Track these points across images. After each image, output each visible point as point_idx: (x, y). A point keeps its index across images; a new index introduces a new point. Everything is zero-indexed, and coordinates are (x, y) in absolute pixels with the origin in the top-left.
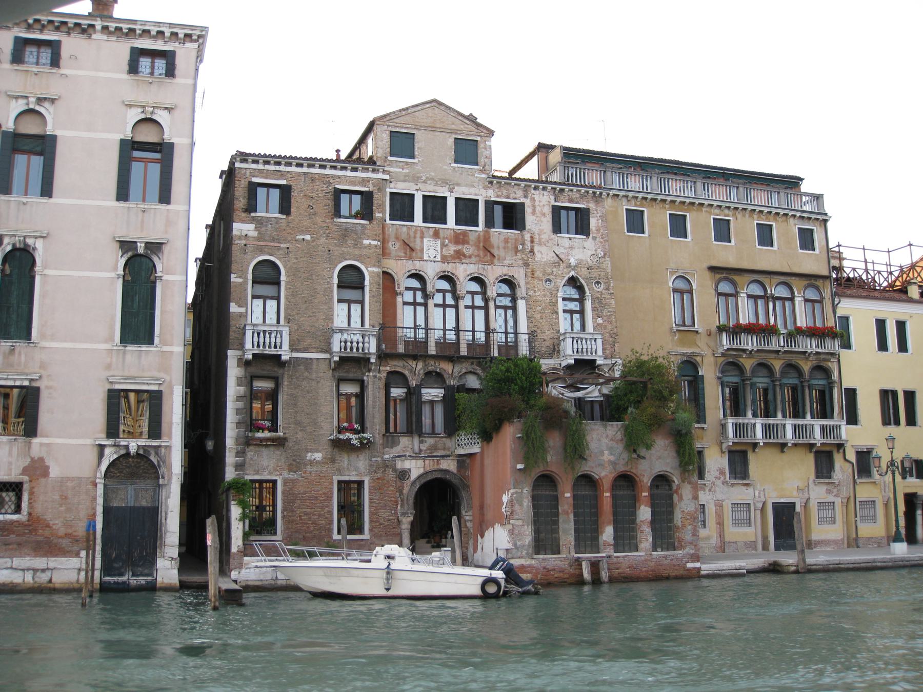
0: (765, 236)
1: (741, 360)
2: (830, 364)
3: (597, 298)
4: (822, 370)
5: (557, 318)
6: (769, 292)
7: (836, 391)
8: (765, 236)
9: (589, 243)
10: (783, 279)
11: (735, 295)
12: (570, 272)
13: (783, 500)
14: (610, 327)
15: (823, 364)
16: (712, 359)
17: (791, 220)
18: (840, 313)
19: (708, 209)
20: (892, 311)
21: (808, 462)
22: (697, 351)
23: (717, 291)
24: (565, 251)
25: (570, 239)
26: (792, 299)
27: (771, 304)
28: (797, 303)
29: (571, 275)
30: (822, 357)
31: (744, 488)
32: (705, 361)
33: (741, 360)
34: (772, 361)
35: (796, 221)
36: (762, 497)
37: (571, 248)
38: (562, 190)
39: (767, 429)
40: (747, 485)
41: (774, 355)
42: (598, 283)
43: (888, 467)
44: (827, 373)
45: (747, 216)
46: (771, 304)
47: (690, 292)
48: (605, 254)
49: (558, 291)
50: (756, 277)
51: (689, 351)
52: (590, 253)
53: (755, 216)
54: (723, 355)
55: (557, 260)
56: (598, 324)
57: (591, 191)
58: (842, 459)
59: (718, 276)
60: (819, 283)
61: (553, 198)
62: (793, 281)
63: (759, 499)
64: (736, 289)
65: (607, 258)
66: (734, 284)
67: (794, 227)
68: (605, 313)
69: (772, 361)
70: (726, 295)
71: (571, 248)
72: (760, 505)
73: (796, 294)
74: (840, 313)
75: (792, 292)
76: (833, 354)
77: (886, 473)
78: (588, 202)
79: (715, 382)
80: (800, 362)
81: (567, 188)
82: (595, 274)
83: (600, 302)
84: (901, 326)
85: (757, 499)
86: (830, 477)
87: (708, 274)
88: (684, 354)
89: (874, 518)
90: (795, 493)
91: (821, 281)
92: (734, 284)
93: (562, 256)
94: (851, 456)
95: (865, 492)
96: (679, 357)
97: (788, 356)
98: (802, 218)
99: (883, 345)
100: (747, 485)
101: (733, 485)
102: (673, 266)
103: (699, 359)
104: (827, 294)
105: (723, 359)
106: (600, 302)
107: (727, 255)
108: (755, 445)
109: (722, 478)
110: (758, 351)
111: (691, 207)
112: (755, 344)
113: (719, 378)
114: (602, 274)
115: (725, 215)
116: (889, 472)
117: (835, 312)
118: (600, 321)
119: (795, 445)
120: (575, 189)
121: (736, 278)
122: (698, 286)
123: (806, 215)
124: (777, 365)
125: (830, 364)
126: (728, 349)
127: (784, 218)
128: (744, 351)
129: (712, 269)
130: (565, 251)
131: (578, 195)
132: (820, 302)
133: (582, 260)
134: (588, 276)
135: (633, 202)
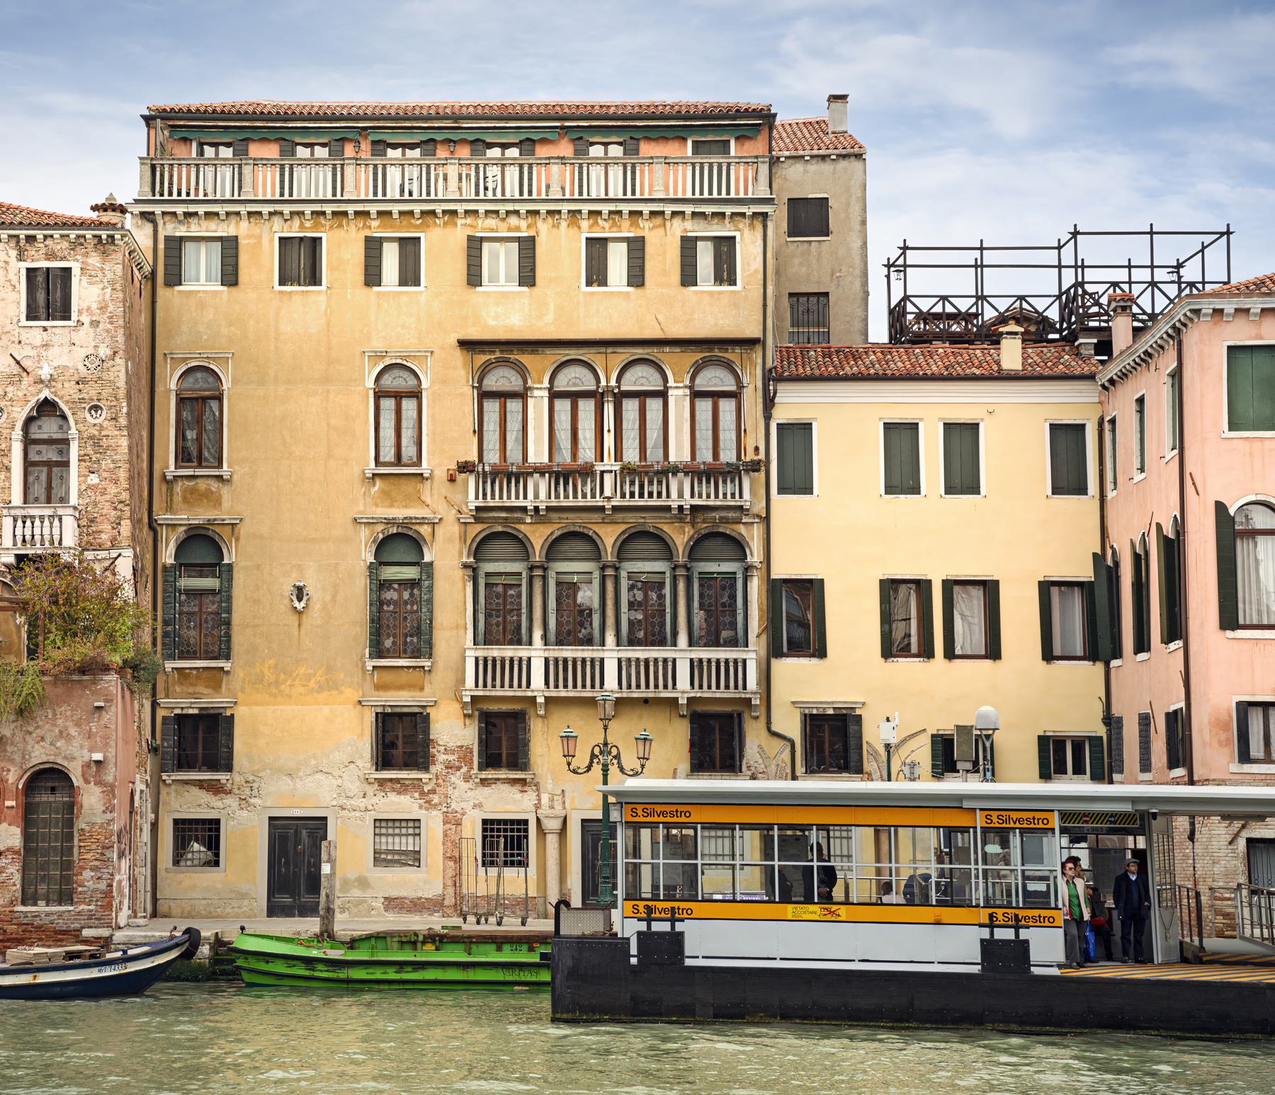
1: (522, 527)
2: (742, 529)
3: (92, 437)
5: (8, 478)
6: (603, 383)
7: (755, 586)
9: (85, 336)
10: (639, 352)
11: (522, 396)
12: (40, 391)
14: (112, 490)
16: (456, 529)
18: (782, 414)
19: (469, 221)
20: (931, 407)
23: (479, 388)
24: (33, 353)
25: (45, 329)
26: (663, 394)
27: (609, 409)
28: (671, 401)
29: (42, 396)
30: (717, 515)
32: (440, 531)
33: (522, 527)
36: (558, 806)
37: (46, 346)
38: (31, 239)
40: (523, 782)
41: (596, 517)
42: (96, 408)
43: (593, 756)
44: (738, 547)
45: (564, 224)
46: (609, 409)
47: (416, 395)
48: (115, 353)
49: (13, 428)
50: (573, 353)
51: (399, 513)
52: (83, 353)
53: (585, 224)
54: (478, 520)
55: (16, 370)
56: (89, 487)
57: (89, 234)
58: (764, 733)
59: (481, 359)
60: (732, 355)
61: (13, 253)
62: (667, 357)
63: (550, 812)
64: (525, 381)
65: (117, 359)
66: (523, 372)
68: (106, 464)
70: (503, 396)
71: (46, 346)
72: (552, 825)
73: (671, 383)
74: (782, 414)
75: (665, 380)
77: (589, 768)
78: (87, 255)
79: (459, 574)
80: (666, 528)
81: (39, 234)
82: (91, 392)
83: (97, 445)
84: (962, 438)
87: (458, 356)
88: (389, 522)
91: (738, 350)
92: (523, 372)
93: (25, 363)
94: (790, 724)
97: (633, 518)
99: (902, 479)
100: (523, 782)
101: (484, 782)
102: (378, 345)
103: (425, 530)
104: (753, 381)
105: (479, 527)
106: (97, 445)
107: (505, 310)
109: (464, 769)
110: (548, 509)
111: (430, 220)
112: (543, 495)
113: (465, 566)
114: (104, 395)
115: (510, 230)
116: (597, 768)
117: (768, 418)
118: (93, 479)
120: (56, 234)
121: (526, 359)
122: (433, 382)
123: (709, 209)
125: (742, 529)
126: (478, 509)
127: (658, 220)
128: (524, 509)
129: (467, 345)
130: (33, 353)
131: (65, 245)
132: (735, 395)
133: (66, 367)
134: (77, 396)
135: (296, 222)
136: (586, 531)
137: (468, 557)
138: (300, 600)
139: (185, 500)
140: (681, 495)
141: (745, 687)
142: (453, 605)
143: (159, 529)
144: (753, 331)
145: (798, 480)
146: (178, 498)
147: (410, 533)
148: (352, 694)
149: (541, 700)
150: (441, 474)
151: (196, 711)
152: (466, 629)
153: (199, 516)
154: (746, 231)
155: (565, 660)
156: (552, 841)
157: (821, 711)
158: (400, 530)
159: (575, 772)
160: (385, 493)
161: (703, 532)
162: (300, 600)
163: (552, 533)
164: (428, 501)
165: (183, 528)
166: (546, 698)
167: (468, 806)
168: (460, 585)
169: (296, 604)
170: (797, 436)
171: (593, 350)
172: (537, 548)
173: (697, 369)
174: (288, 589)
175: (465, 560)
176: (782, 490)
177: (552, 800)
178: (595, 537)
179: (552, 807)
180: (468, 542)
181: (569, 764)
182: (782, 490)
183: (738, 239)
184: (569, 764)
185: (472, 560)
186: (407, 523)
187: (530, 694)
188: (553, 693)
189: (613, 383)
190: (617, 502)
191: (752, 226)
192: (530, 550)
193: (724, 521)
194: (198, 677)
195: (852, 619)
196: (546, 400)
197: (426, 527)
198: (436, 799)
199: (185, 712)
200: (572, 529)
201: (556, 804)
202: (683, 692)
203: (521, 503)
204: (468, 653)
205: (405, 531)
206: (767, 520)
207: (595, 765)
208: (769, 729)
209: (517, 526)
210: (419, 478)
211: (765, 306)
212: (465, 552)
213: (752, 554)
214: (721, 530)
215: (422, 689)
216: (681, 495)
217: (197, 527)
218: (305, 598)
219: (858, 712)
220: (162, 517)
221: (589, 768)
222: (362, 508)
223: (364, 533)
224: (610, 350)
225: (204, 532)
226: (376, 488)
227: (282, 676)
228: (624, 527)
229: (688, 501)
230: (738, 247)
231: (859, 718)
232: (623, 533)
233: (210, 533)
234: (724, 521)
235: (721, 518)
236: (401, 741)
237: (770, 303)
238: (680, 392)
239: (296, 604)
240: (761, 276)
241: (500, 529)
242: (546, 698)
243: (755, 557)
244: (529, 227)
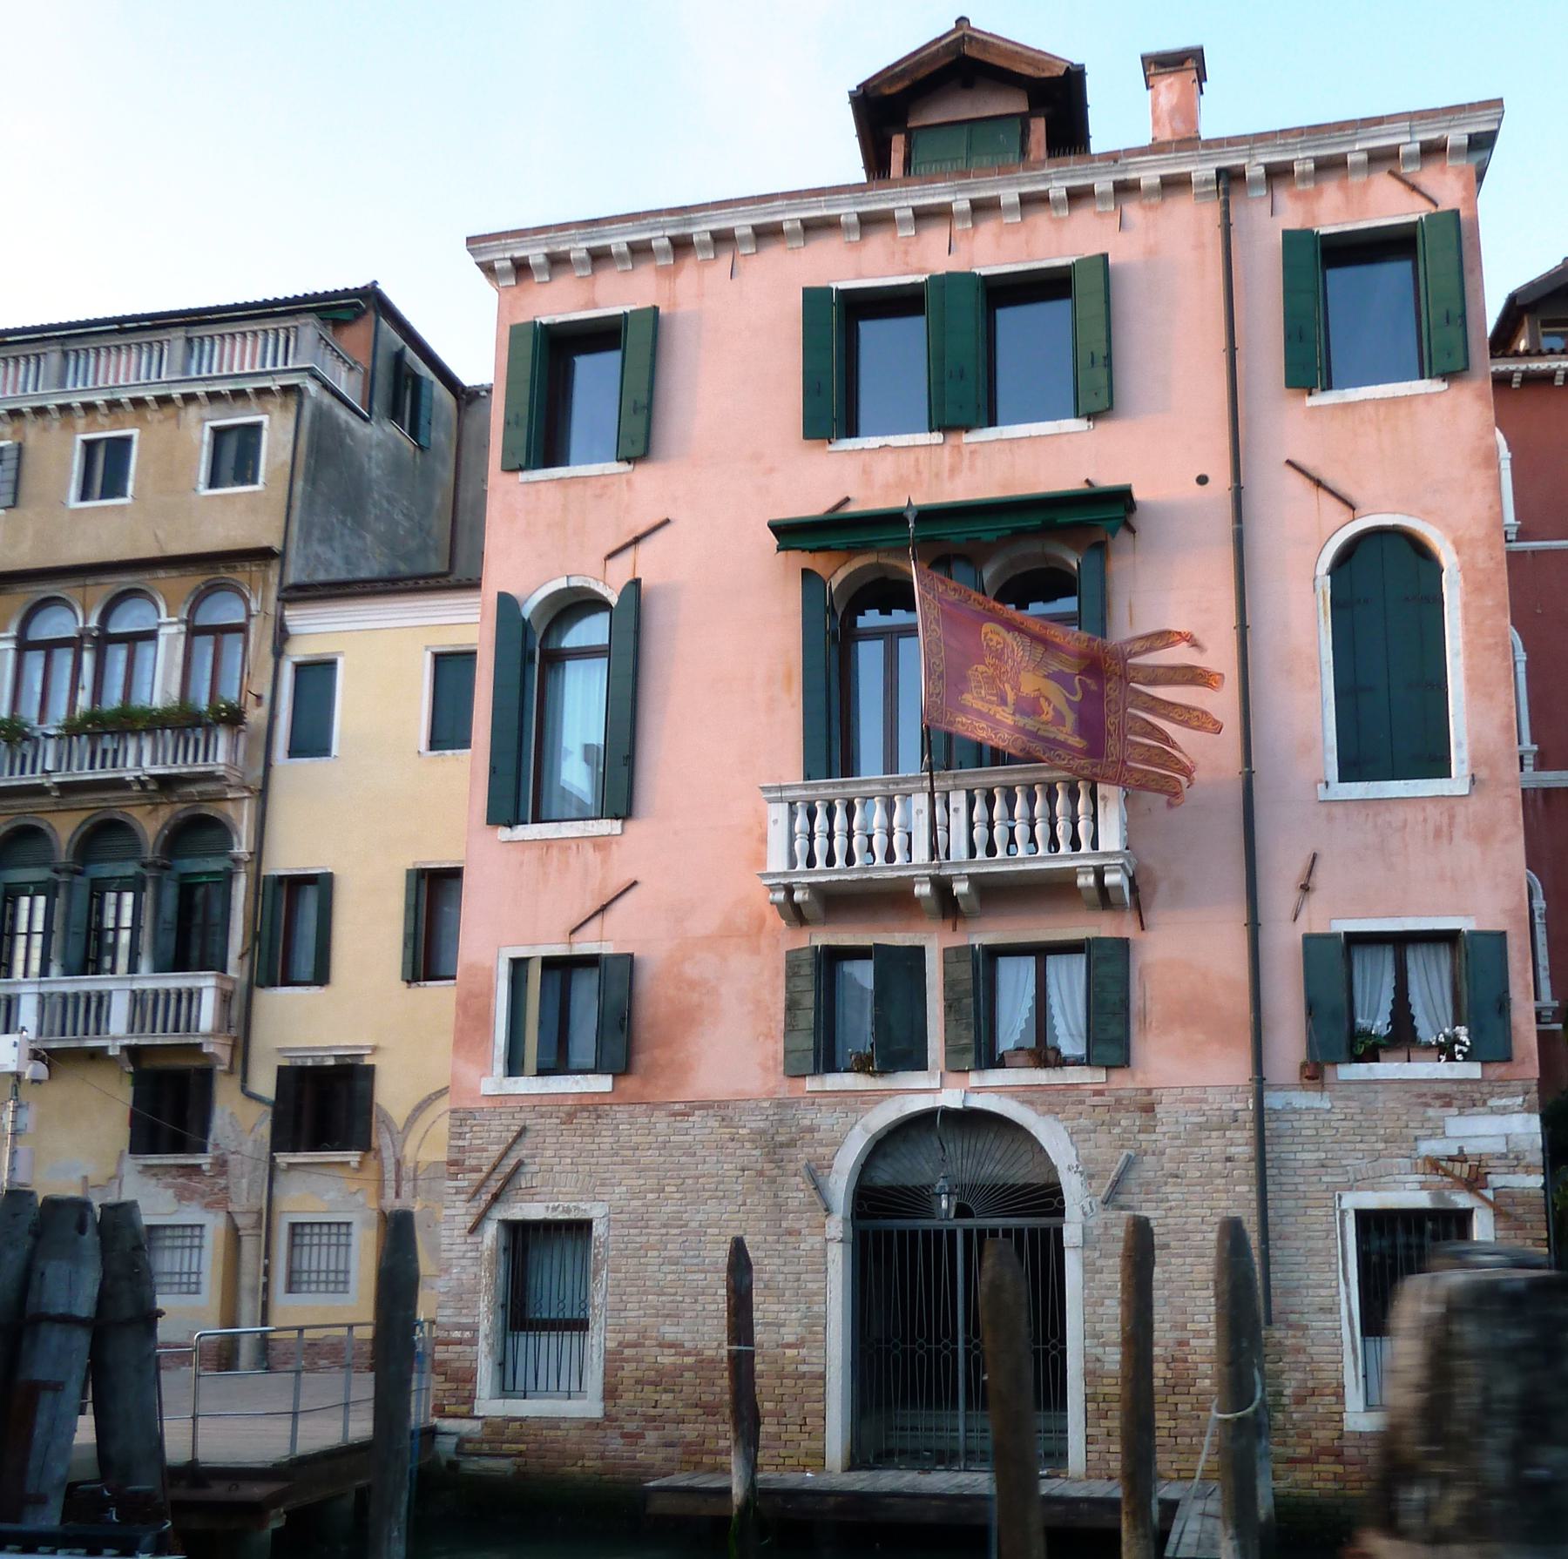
0: (106, 469)
2: (229, 808)
4: (199, 830)
7: (240, 888)
8: (106, 469)
15: (209, 810)
17: (193, 412)
18: (299, 651)
21: (108, 1108)
27: (88, 659)
30: (193, 789)
34: (49, 818)
35: (207, 411)
46: (88, 659)
53: (81, 423)
58: (239, 1096)
67: (199, 428)
74: (299, 651)
89: (338, 1281)
95: (322, 1190)
98: (213, 397)
117: (278, 653)
123: (224, 387)
127: (169, 410)
140: (139, 763)
144: (272, 540)
145: (312, 738)
154: (277, 413)
157: (318, 1062)
170: (316, 678)
171: (72, 583)
173: (200, 598)
183: (266, 425)
189: (93, 623)
191: (284, 406)
195: (369, 929)
196: (11, 656)
202: (114, 1038)
208: (243, 1089)
211: (289, 507)
213: (240, 843)
214: (204, 811)
216: (139, 763)
219: (367, 1061)
224: (90, 581)
228: (84, 815)
230: (265, 435)
231: (370, 1071)
232: (83, 823)
235: (201, 793)
237: (297, 503)
238: (173, 630)
240: (288, 470)
243: (242, 846)
244: (15, 432)
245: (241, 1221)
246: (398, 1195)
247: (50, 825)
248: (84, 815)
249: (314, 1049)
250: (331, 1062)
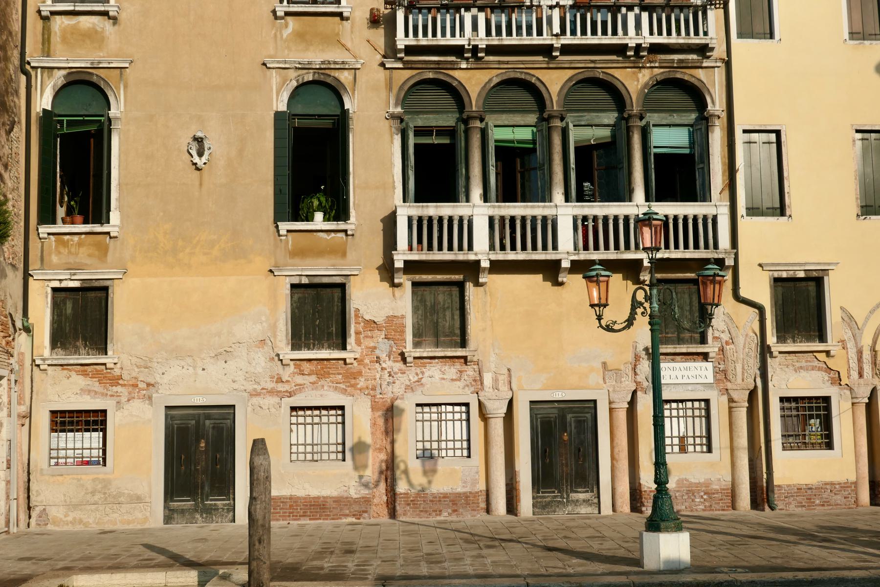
1: (456, 74)
2: (701, 74)
13: (559, 396)
22: (335, 55)
31: (451, 370)
33: (456, 74)
34: (538, 74)
39: (505, 231)
44: (696, 96)
51: (316, 56)
69: (538, 74)
76: (703, 50)
77: (630, 322)
80: (617, 73)
85: (487, 394)
86: (703, 340)
88: (305, 67)
90: (596, 378)
96: (292, 74)
103: (345, 77)
105: (408, 73)
108: (472, 269)
113: (393, 117)
119: (578, 267)
124: (554, 81)
125: (701, 74)
128: (458, 51)
136: (528, 78)
137: (396, 105)
138: (200, 154)
139: (64, 39)
141: (716, 246)
142: (377, 163)
143: (33, 73)
146: (56, 39)
147: (329, 80)
148: (262, 263)
149: (485, 264)
150: (361, 16)
151: (76, 284)
152: (394, 188)
153: (81, 60)
155: (513, 219)
156: (497, 428)
158: (317, 77)
159: (609, 329)
160: (300, 36)
161: (659, 78)
162: (200, 154)
163: (490, 80)
164: (349, 45)
165: (64, 72)
166: (491, 262)
167: (398, 389)
168: (387, 137)
169: (196, 159)
172: (474, 96)
174: (185, 139)
175: (391, 110)
176: (740, 35)
177: (496, 380)
178: (538, 84)
179: (496, 388)
180: (395, 90)
181: (599, 318)
182: (740, 35)
184: (599, 318)
185: (399, 110)
186: (325, 68)
187: (472, 257)
188: (500, 256)
190: (568, 40)
192: (466, 99)
193: (683, 65)
194: (80, 244)
197: (346, 73)
198: (362, 383)
199: (65, 284)
200: (512, 75)
201: (501, 383)
203: (457, 41)
204: (399, 212)
205: (322, 78)
206: (728, 64)
207: (639, 317)
208: (737, 297)
209: (451, 72)
210: (338, 19)
212: (392, 101)
214: (678, 76)
215: (344, 255)
217: (80, 71)
218: (206, 153)
220: (34, 58)
221: (630, 322)
222: (272, 52)
223: (274, 78)
225: (87, 78)
226: (290, 29)
227: (180, 243)
228: (571, 73)
229: (647, 39)
232: (570, 79)
233: (94, 79)
234: (683, 65)
236: (320, 314)
239: (196, 159)
241: (431, 75)
242: (491, 262)
243: (716, 105)
245: (735, 395)
246: (861, 375)
247: (538, 79)
248: (571, 73)
249: (805, 264)
250: (802, 275)
